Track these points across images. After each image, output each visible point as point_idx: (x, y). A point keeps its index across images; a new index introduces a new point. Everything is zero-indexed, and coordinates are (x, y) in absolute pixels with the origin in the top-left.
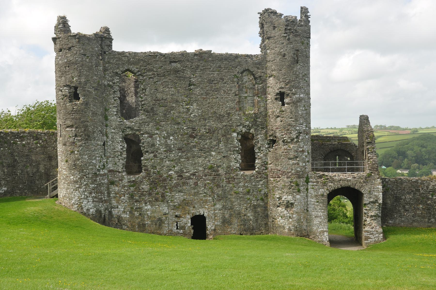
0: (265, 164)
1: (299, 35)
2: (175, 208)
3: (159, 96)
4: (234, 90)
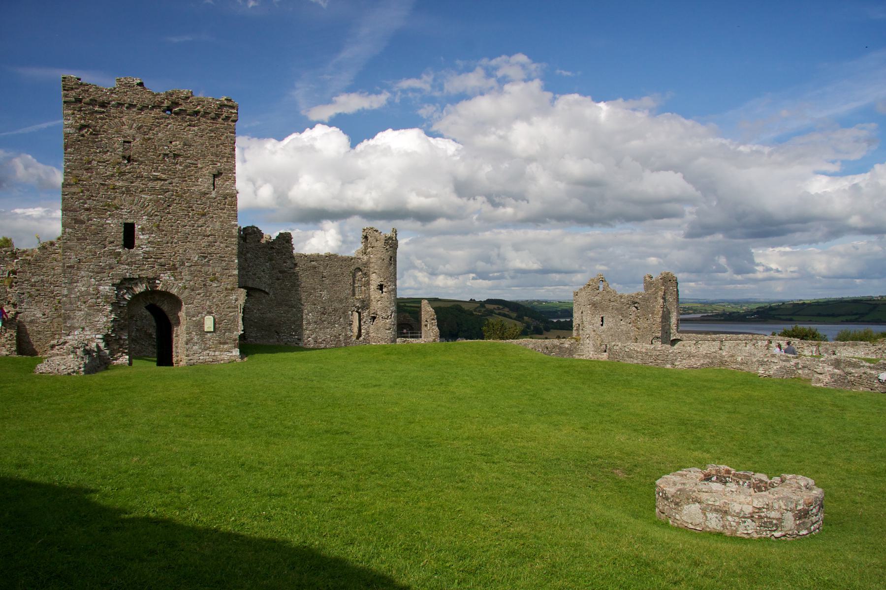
0: (368, 333)
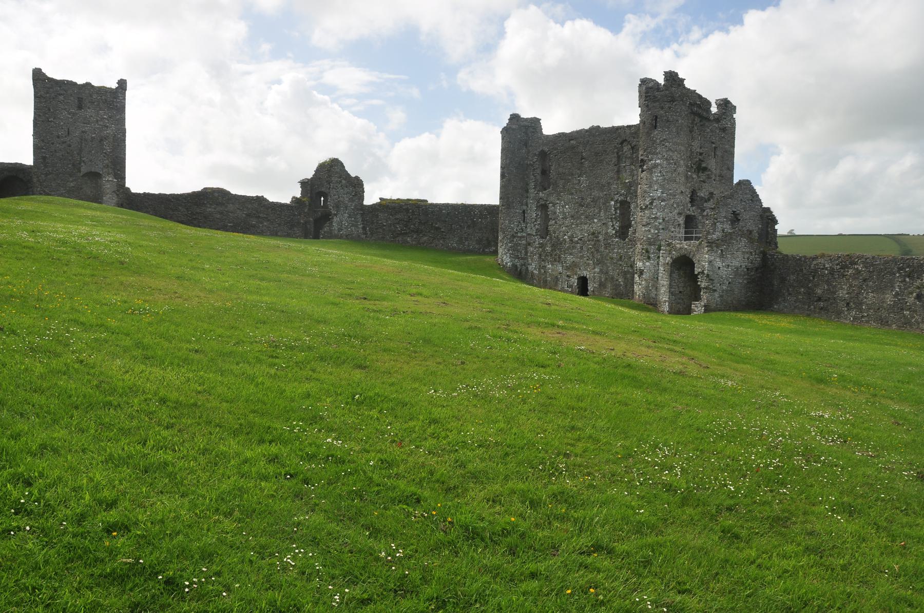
1: (658, 101)
2: (568, 268)
3: (561, 170)
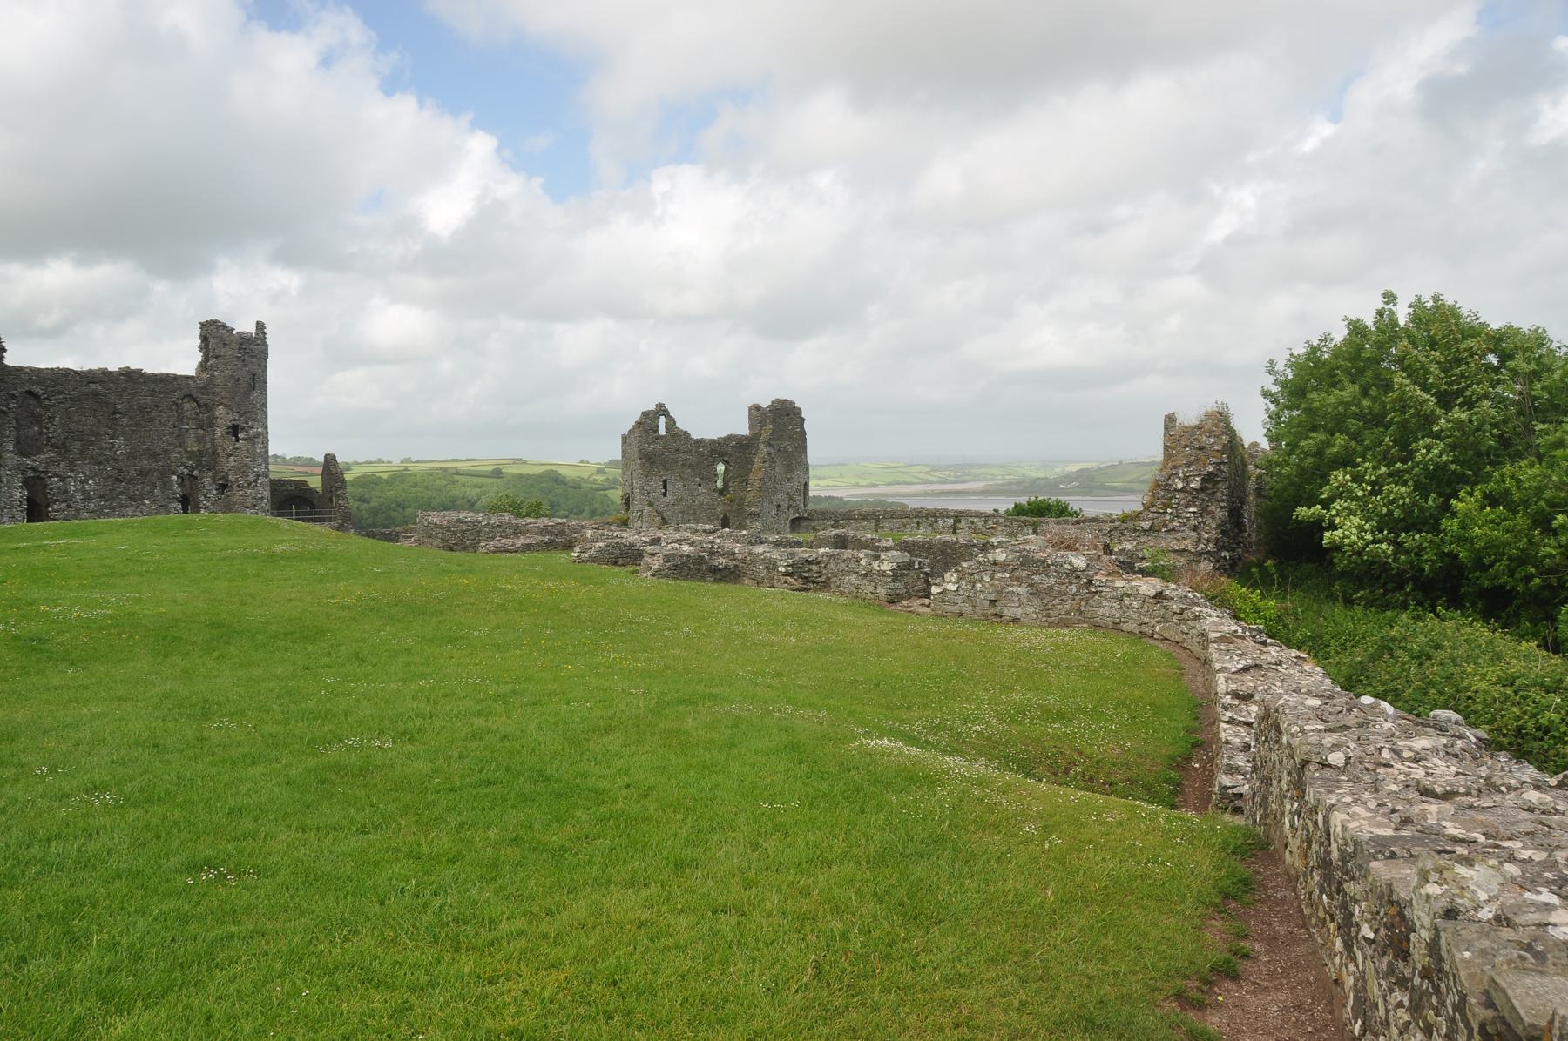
4: (172, 420)
